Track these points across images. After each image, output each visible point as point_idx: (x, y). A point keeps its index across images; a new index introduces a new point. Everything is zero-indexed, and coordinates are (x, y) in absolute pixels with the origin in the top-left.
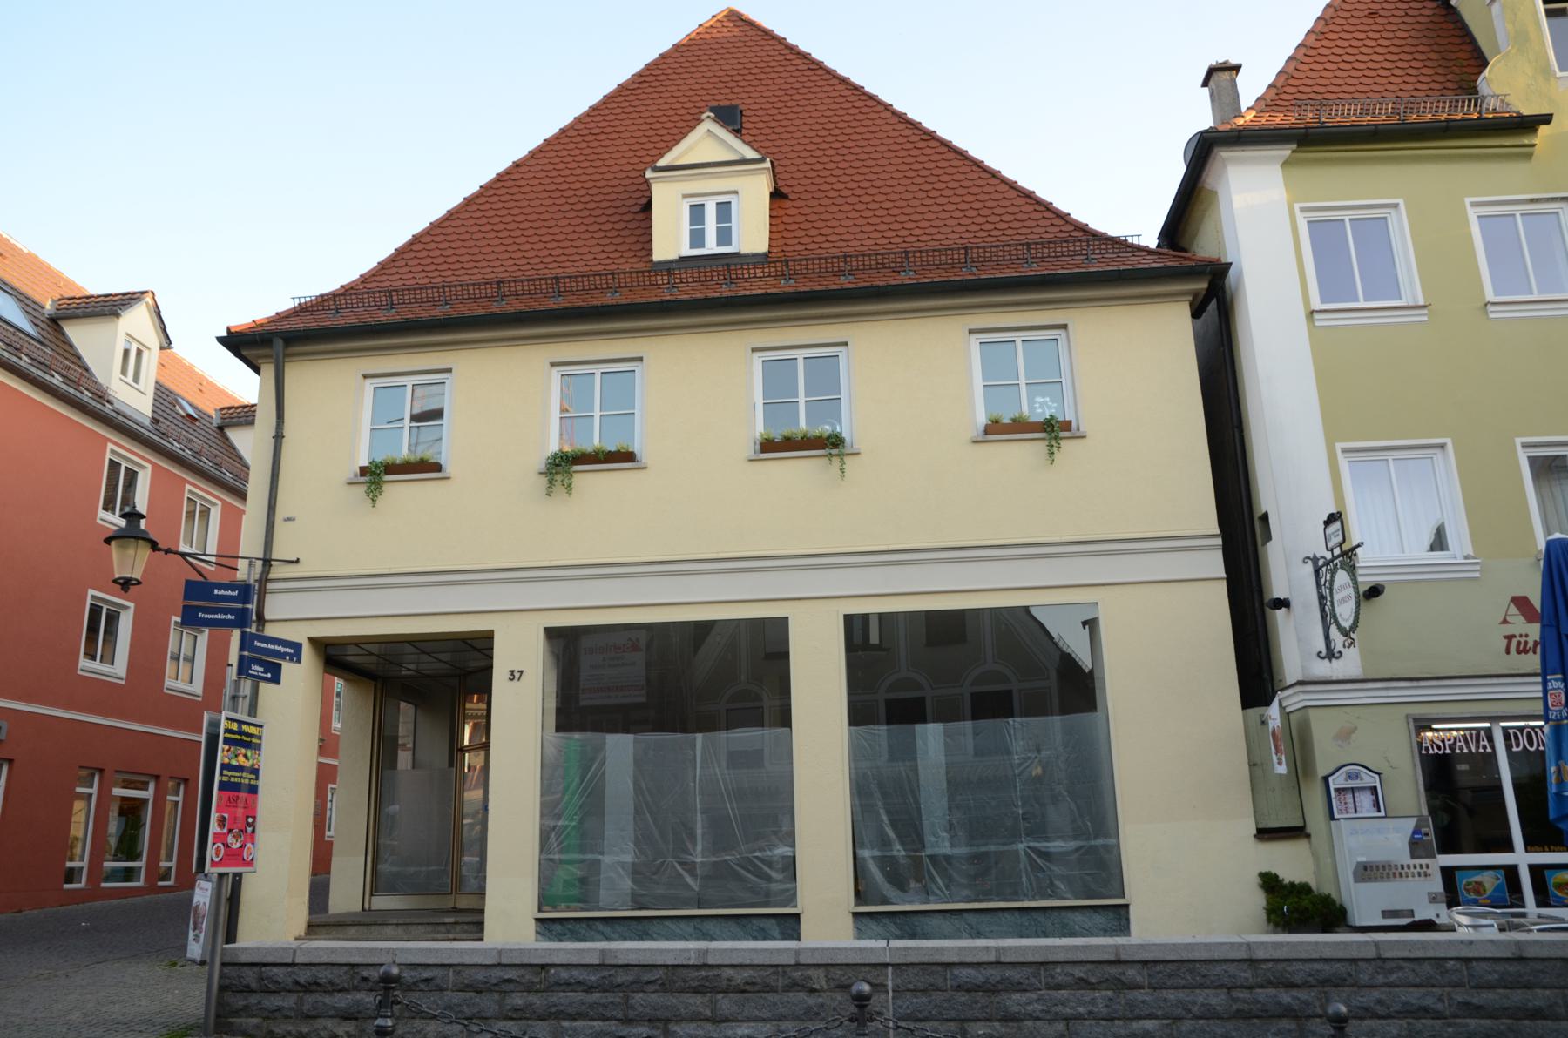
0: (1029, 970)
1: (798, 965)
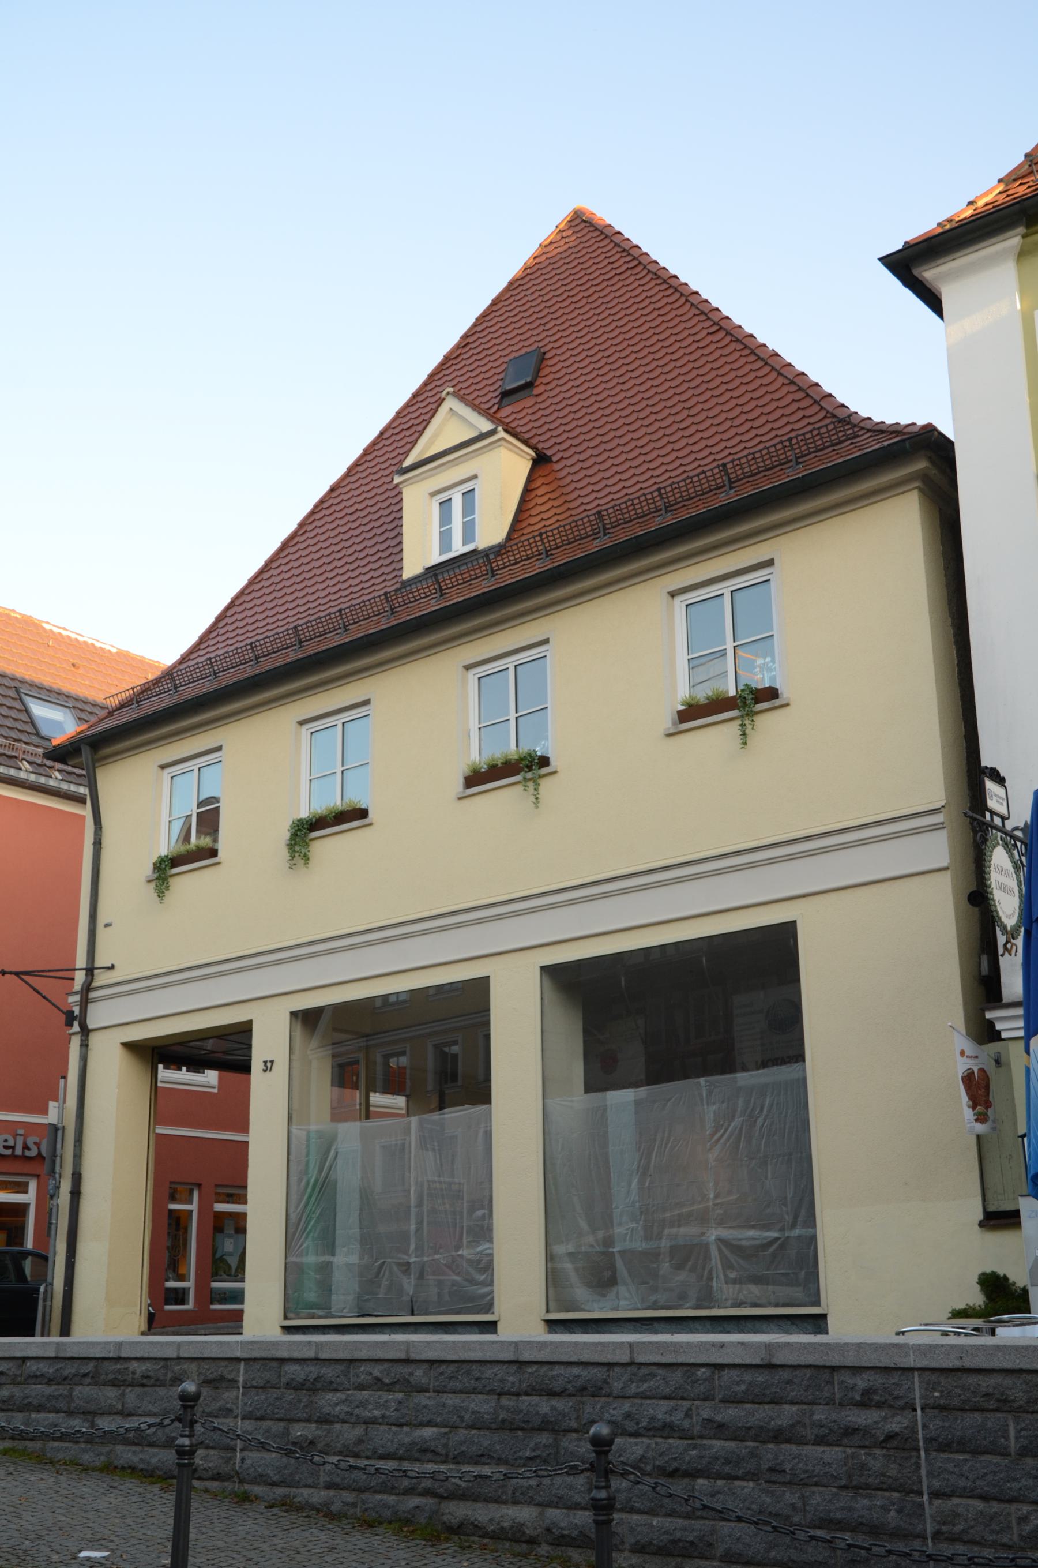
0: (340, 1368)
1: (179, 1358)
